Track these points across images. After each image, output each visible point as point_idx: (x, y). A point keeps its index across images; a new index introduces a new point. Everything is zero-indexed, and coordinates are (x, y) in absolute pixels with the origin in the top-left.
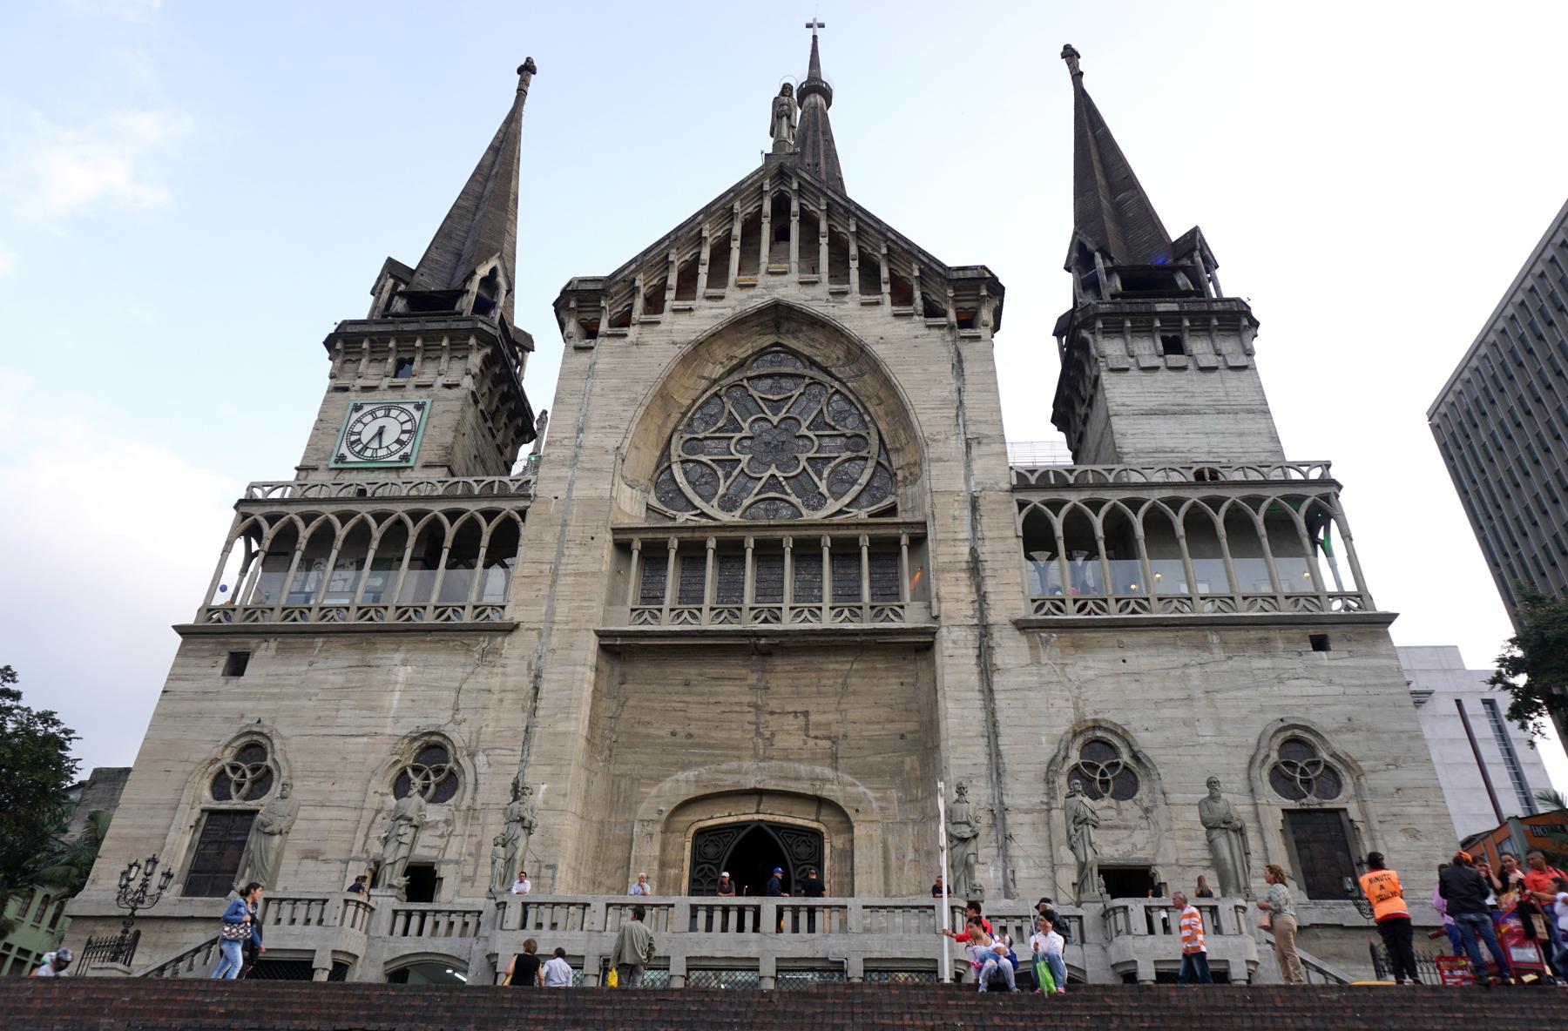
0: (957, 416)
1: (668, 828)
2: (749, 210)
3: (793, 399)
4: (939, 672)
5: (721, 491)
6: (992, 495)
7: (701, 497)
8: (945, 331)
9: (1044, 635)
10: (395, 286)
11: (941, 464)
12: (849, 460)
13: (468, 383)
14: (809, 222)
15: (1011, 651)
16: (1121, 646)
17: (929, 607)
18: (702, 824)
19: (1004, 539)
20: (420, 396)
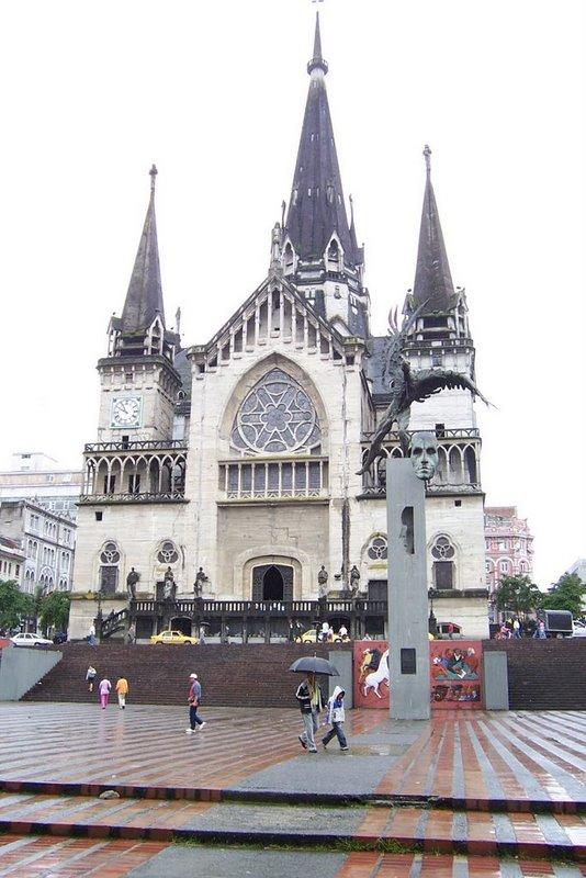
13: (156, 386)
14: (288, 306)
15: (355, 507)
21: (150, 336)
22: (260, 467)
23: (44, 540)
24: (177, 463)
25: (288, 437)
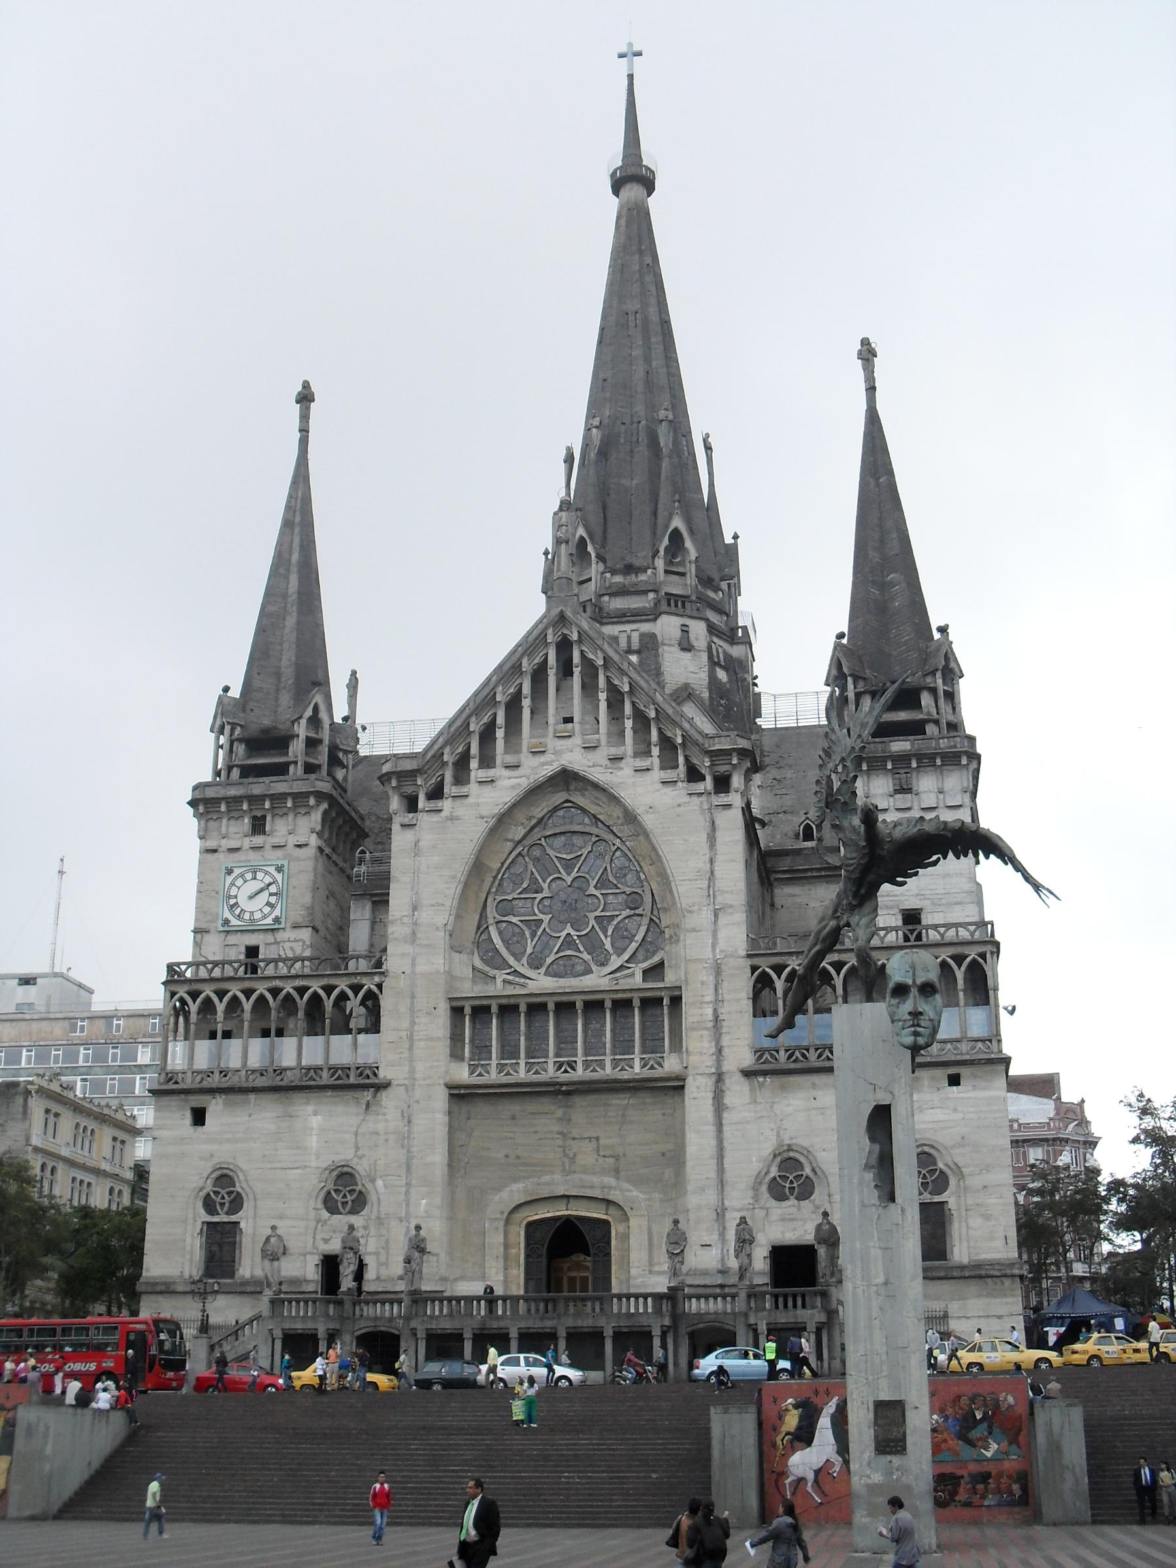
0: (709, 887)
1: (507, 1222)
2: (536, 661)
3: (583, 858)
4: (687, 1109)
5: (529, 950)
6: (732, 962)
7: (514, 955)
8: (704, 798)
9: (761, 1079)
11: (694, 933)
13: (314, 841)
14: (590, 669)
16: (814, 1086)
18: (530, 1219)
19: (738, 1000)
20: (276, 857)
21: (302, 736)
22: (537, 1008)
23: (71, 1163)
24: (363, 1003)
25: (594, 945)
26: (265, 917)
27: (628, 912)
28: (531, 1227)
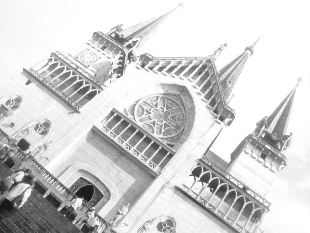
5: (142, 116)
7: (137, 115)
10: (116, 31)
12: (173, 130)
17: (161, 170)
26: (87, 63)
27: (174, 128)
28: (81, 178)
